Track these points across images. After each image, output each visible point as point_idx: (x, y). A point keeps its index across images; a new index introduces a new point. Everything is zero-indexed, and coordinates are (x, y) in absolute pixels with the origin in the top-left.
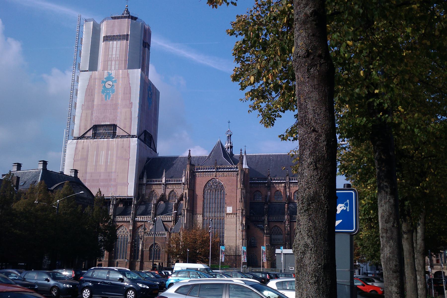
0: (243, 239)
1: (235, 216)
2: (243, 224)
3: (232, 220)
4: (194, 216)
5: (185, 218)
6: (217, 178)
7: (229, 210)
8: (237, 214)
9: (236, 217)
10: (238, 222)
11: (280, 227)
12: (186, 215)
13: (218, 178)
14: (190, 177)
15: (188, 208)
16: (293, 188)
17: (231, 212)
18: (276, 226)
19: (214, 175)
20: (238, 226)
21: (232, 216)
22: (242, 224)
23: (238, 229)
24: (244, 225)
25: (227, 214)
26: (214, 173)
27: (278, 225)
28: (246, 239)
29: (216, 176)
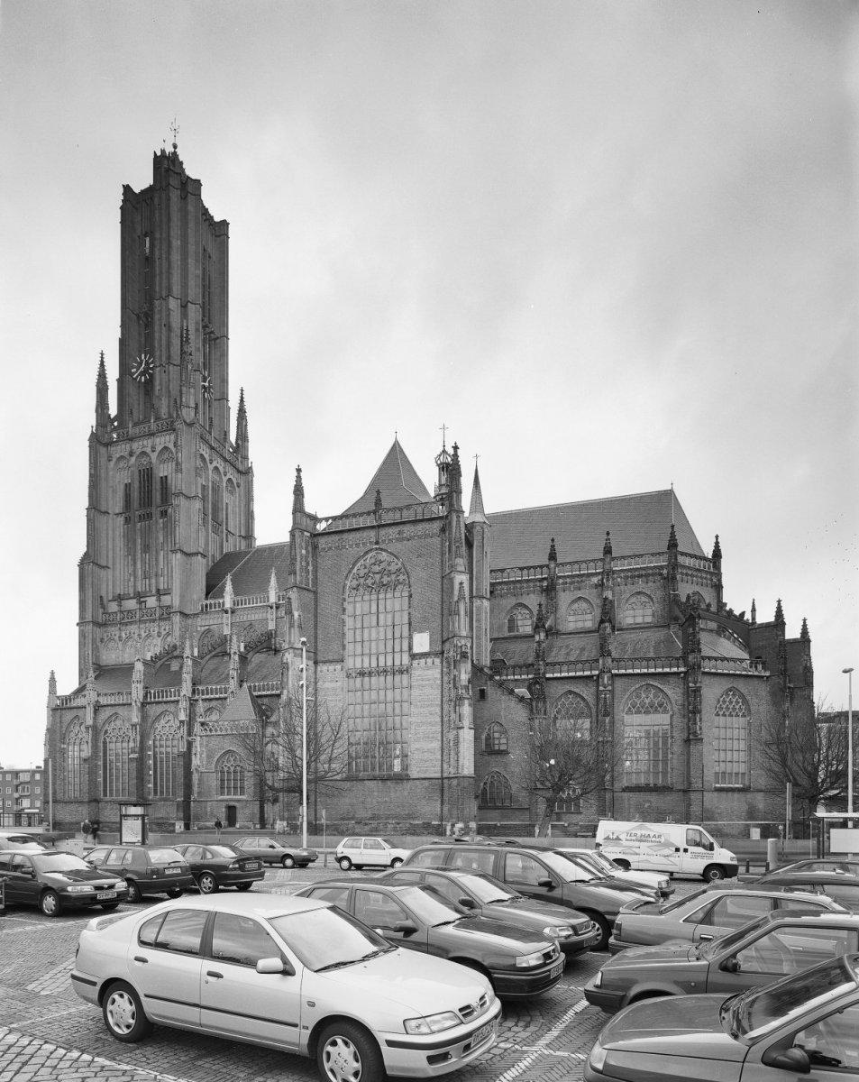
1: (437, 661)
3: (430, 672)
4: (319, 668)
6: (382, 549)
8: (443, 653)
10: (446, 678)
11: (581, 693)
14: (304, 552)
17: (426, 649)
18: (570, 692)
21: (429, 661)
25: (413, 656)
27: (576, 690)
28: (471, 729)
29: (377, 543)
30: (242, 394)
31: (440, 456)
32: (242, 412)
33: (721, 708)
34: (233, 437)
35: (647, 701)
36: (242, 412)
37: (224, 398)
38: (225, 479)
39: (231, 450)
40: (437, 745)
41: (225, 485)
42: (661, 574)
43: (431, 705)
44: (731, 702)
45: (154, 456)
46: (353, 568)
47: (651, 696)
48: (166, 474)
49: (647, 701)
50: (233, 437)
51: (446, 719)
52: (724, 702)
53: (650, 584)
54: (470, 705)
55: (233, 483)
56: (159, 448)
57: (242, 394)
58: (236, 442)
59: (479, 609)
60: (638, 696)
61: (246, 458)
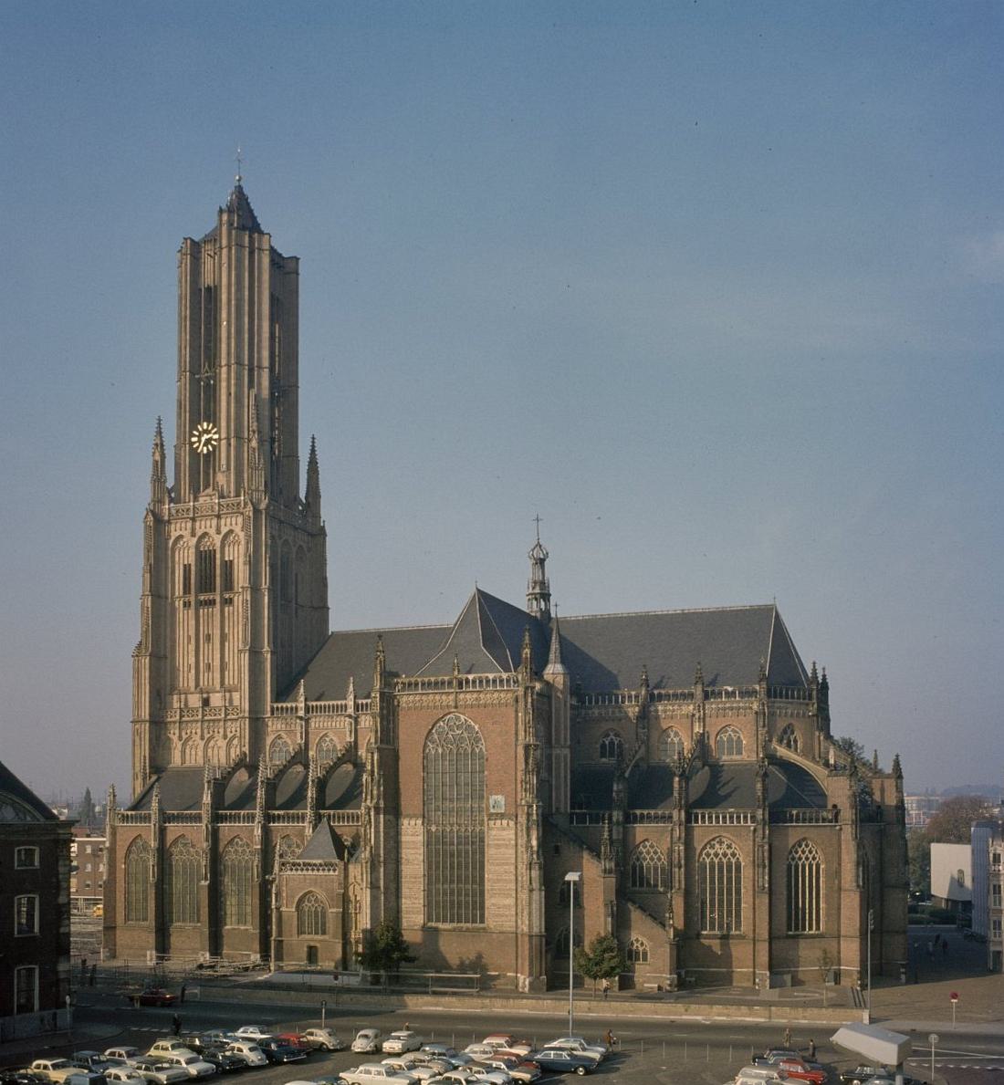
0: (531, 891)
1: (512, 823)
2: (532, 847)
3: (505, 833)
5: (373, 830)
7: (498, 801)
9: (516, 824)
12: (373, 820)
13: (461, 711)
15: (377, 803)
16: (713, 720)
19: (452, 703)
20: (519, 854)
22: (528, 846)
23: (519, 859)
24: (535, 849)
26: (452, 697)
30: (313, 442)
31: (533, 550)
32: (313, 463)
33: (793, 859)
34: (302, 495)
35: (720, 852)
36: (313, 463)
37: (294, 456)
38: (294, 549)
39: (300, 508)
40: (511, 901)
41: (294, 554)
42: (751, 708)
43: (507, 864)
44: (803, 852)
45: (218, 539)
46: (432, 729)
47: (724, 846)
48: (231, 558)
49: (720, 852)
50: (302, 495)
51: (520, 879)
52: (797, 853)
53: (740, 717)
54: (540, 868)
55: (303, 548)
56: (224, 530)
57: (313, 442)
58: (306, 498)
59: (558, 757)
60: (712, 847)
61: (317, 516)
